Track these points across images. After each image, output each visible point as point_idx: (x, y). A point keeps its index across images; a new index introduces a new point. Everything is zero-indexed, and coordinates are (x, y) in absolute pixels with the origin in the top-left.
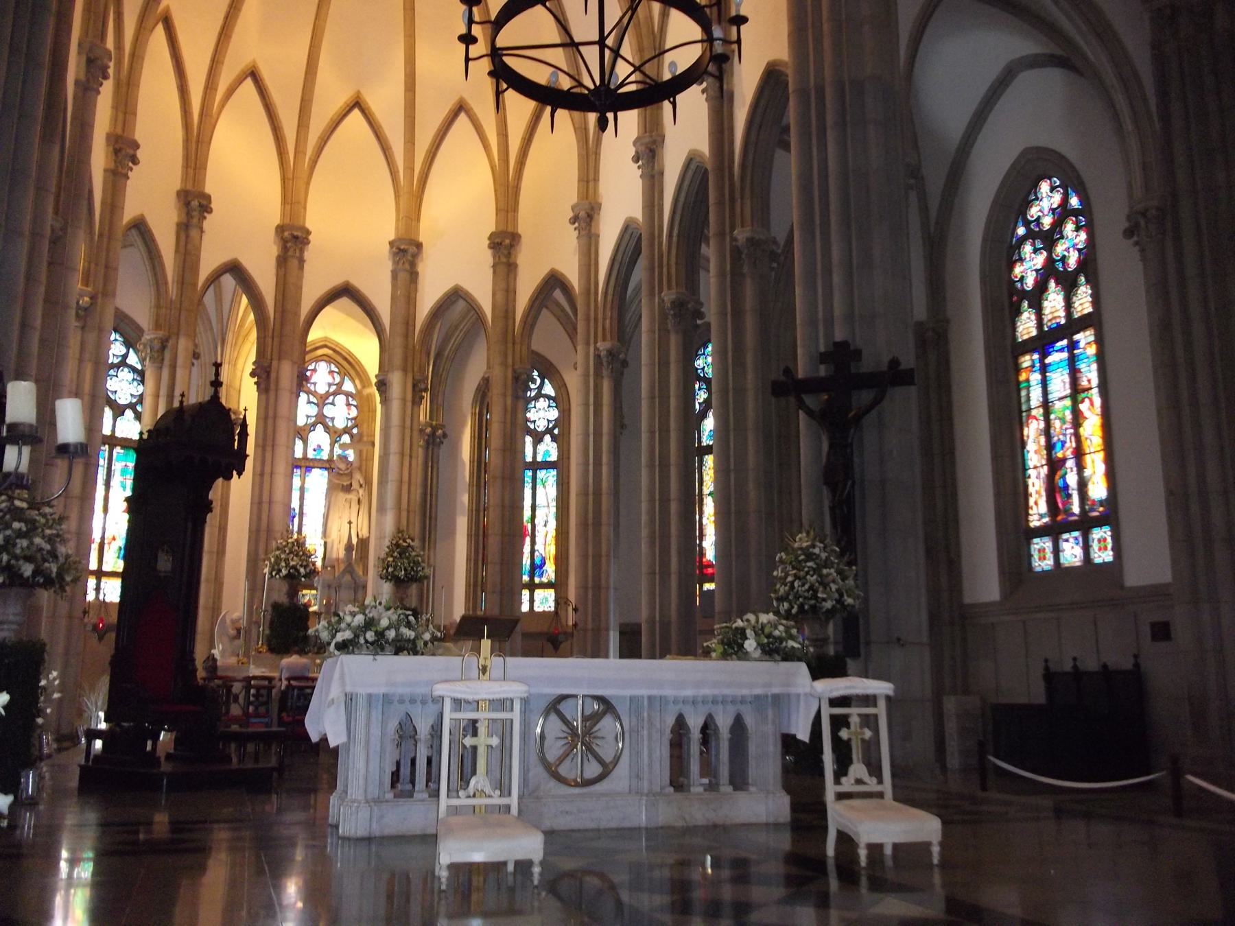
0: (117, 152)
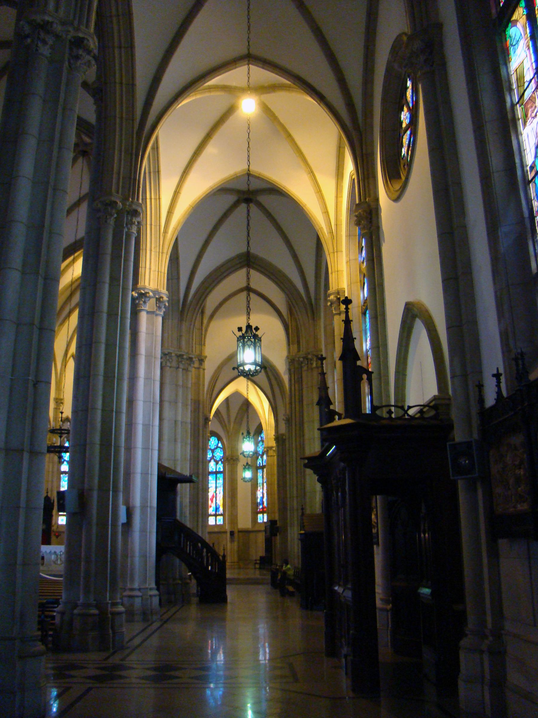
0: (57, 402)
